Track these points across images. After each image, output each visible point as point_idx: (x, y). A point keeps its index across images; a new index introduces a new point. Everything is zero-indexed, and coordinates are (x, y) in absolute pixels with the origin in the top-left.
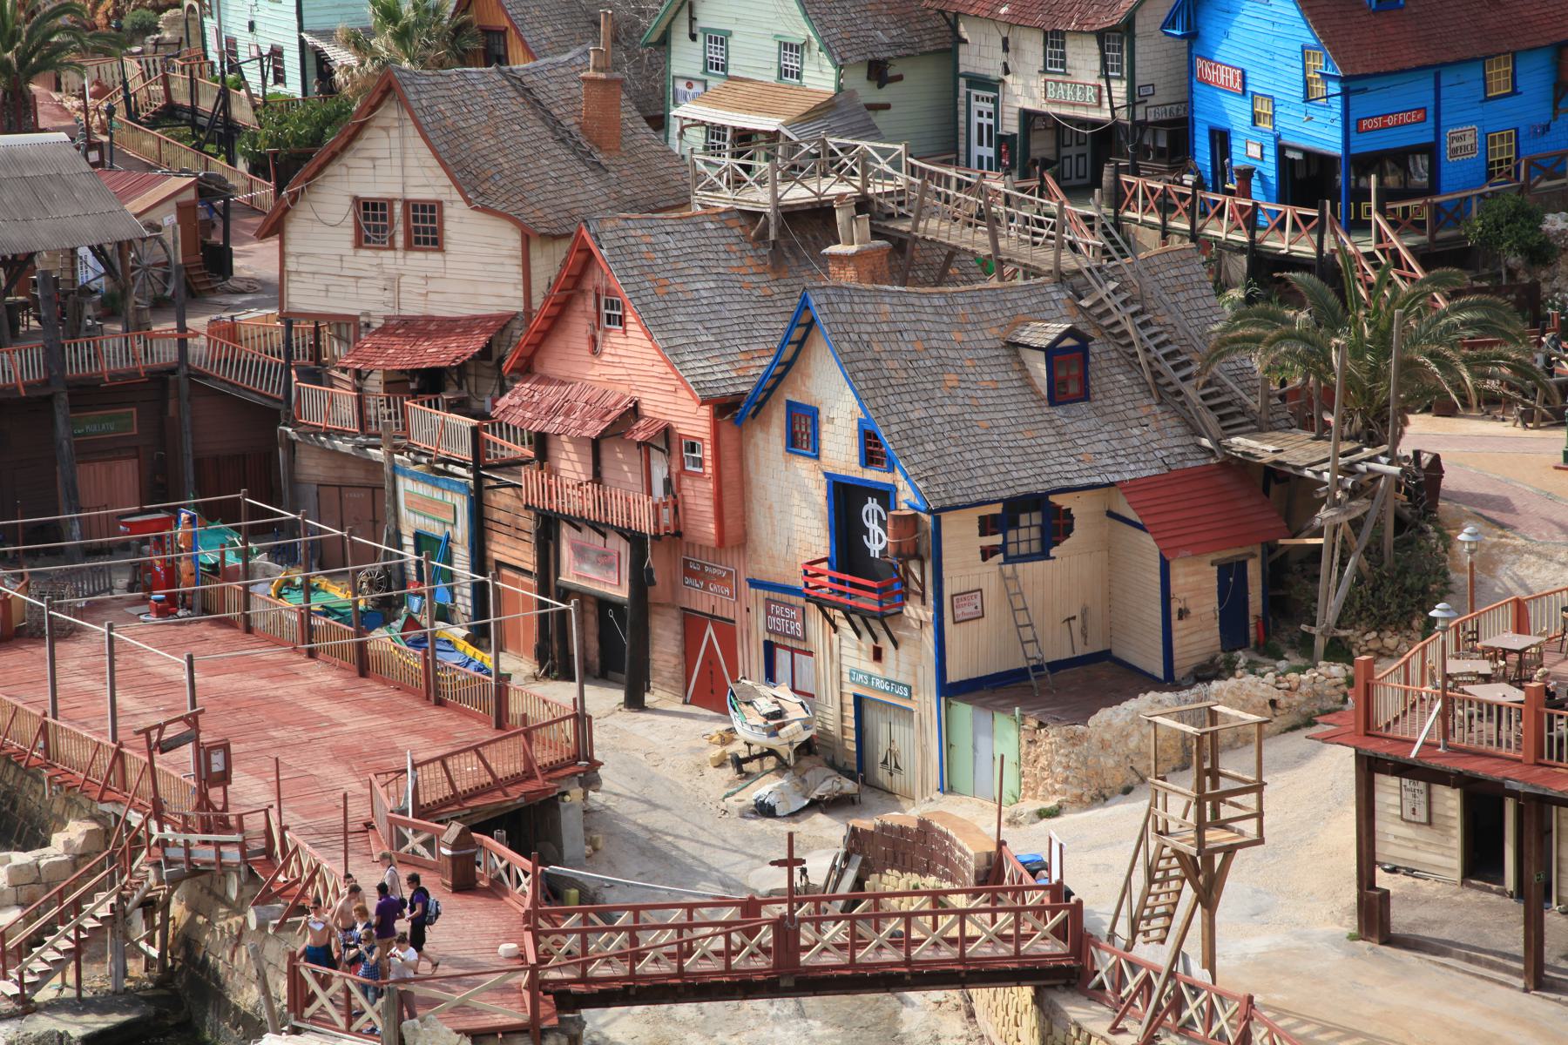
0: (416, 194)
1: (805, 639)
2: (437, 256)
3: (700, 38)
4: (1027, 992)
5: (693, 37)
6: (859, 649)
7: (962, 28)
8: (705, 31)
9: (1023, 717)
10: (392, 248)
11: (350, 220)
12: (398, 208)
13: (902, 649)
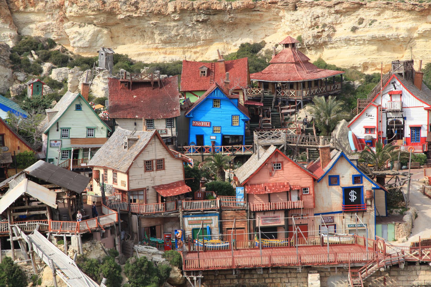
0: (158, 158)
1: (333, 222)
2: (163, 171)
3: (60, 130)
5: (58, 130)
6: (351, 220)
7: (116, 122)
8: (61, 128)
9: (395, 223)
10: (153, 171)
11: (144, 167)
12: (154, 162)
13: (364, 217)
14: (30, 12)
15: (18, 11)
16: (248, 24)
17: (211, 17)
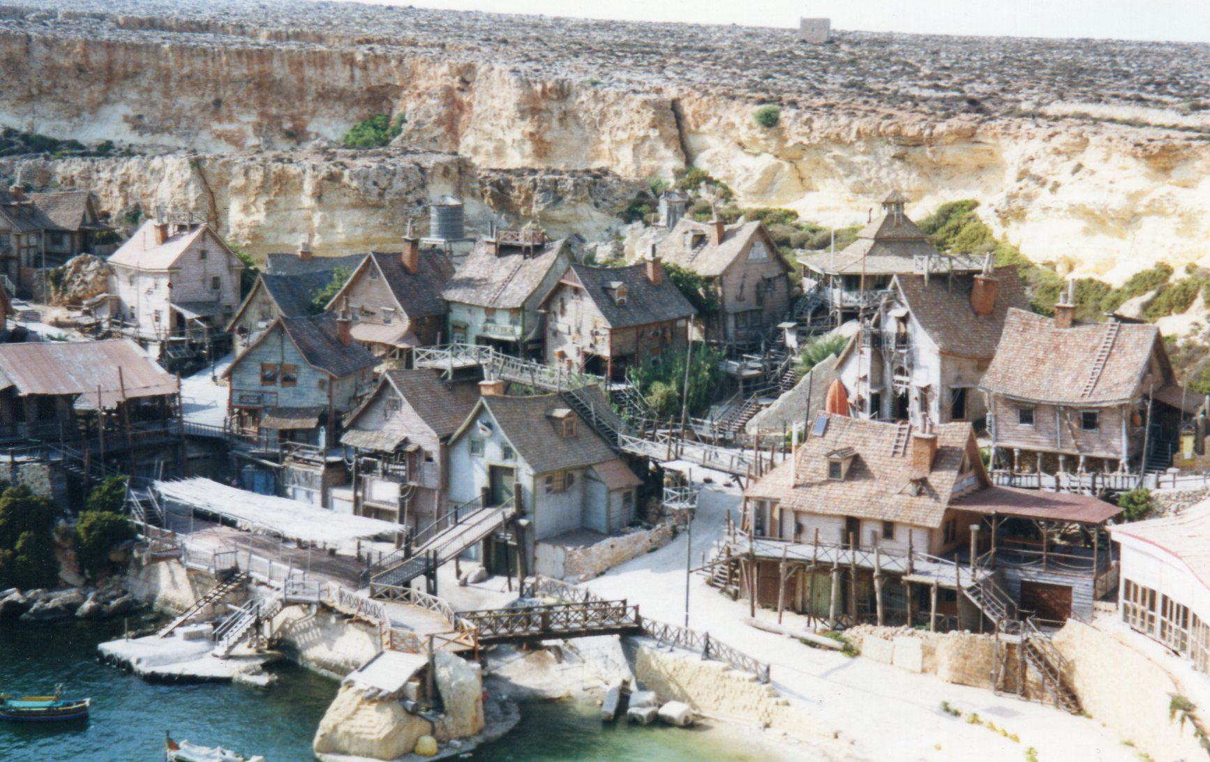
4: (617, 637)
14: (704, 133)
15: (690, 131)
16: (981, 168)
17: (911, 150)
